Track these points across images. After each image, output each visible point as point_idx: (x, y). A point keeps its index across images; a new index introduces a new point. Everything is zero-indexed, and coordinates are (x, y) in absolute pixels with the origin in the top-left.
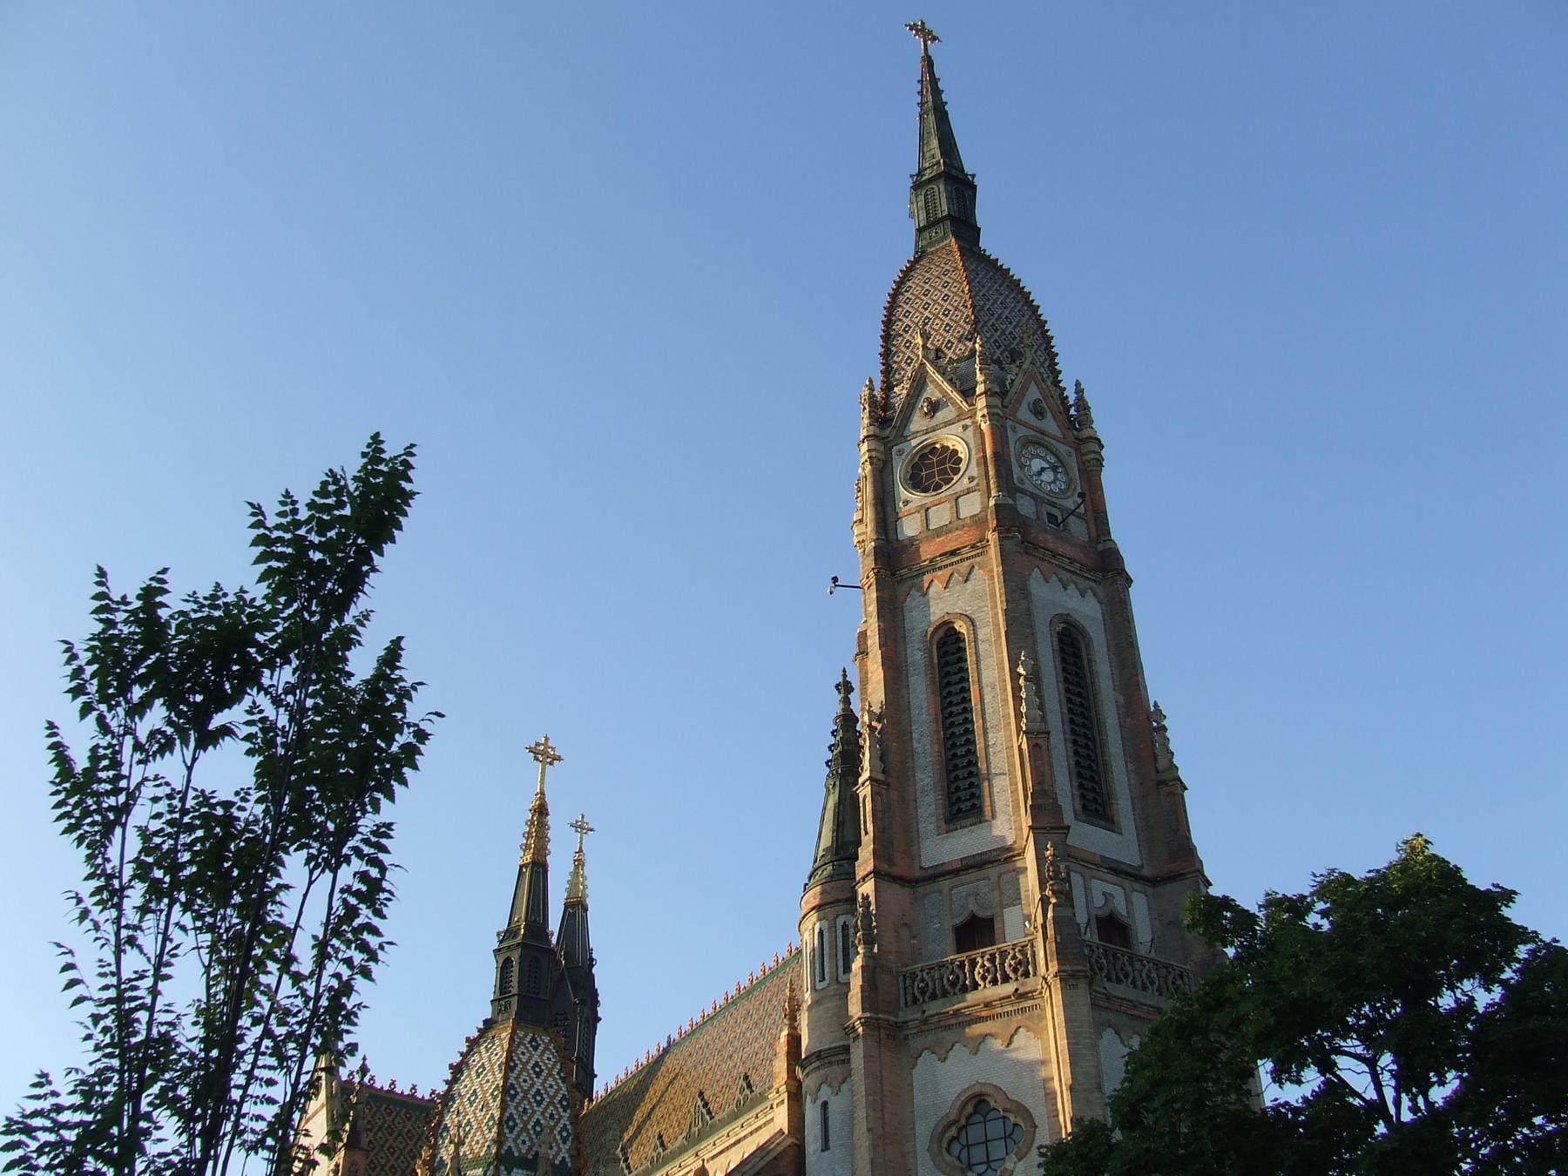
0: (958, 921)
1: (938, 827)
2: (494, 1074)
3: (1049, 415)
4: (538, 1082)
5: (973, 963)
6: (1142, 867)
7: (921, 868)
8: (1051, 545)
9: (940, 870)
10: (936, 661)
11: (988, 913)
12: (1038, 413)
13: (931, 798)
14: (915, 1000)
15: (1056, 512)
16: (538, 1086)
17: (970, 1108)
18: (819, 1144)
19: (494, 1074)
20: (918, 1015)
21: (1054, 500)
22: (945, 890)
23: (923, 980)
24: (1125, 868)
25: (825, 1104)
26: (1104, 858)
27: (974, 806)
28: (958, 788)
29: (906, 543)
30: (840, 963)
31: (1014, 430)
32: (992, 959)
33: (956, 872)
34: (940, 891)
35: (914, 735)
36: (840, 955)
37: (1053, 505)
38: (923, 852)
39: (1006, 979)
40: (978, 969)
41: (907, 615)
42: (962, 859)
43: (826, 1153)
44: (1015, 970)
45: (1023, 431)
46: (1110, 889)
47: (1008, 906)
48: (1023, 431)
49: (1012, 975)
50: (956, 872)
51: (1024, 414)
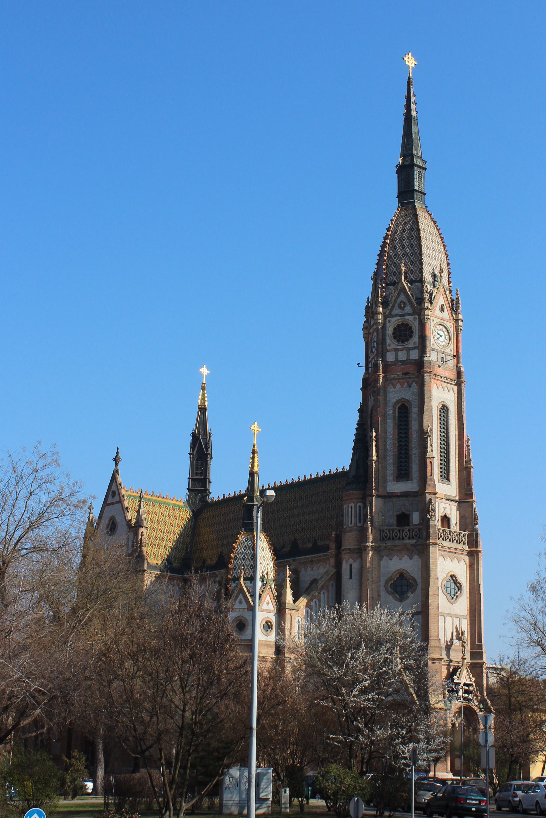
0: (398, 513)
1: (394, 479)
2: (250, 550)
4: (263, 553)
5: (403, 531)
6: (456, 496)
7: (387, 492)
10: (397, 415)
11: (408, 513)
12: (442, 310)
15: (444, 356)
16: (263, 555)
18: (348, 577)
19: (250, 550)
21: (443, 350)
22: (395, 502)
23: (386, 533)
24: (452, 498)
25: (351, 565)
26: (445, 495)
27: (406, 473)
28: (401, 465)
29: (390, 363)
30: (358, 520)
31: (433, 321)
32: (409, 531)
34: (393, 502)
35: (388, 443)
36: (358, 517)
37: (443, 353)
38: (388, 487)
39: (413, 538)
40: (404, 533)
41: (388, 394)
42: (401, 492)
43: (351, 580)
44: (416, 536)
45: (437, 320)
46: (445, 505)
47: (414, 512)
48: (437, 320)
49: (415, 537)
51: (437, 312)
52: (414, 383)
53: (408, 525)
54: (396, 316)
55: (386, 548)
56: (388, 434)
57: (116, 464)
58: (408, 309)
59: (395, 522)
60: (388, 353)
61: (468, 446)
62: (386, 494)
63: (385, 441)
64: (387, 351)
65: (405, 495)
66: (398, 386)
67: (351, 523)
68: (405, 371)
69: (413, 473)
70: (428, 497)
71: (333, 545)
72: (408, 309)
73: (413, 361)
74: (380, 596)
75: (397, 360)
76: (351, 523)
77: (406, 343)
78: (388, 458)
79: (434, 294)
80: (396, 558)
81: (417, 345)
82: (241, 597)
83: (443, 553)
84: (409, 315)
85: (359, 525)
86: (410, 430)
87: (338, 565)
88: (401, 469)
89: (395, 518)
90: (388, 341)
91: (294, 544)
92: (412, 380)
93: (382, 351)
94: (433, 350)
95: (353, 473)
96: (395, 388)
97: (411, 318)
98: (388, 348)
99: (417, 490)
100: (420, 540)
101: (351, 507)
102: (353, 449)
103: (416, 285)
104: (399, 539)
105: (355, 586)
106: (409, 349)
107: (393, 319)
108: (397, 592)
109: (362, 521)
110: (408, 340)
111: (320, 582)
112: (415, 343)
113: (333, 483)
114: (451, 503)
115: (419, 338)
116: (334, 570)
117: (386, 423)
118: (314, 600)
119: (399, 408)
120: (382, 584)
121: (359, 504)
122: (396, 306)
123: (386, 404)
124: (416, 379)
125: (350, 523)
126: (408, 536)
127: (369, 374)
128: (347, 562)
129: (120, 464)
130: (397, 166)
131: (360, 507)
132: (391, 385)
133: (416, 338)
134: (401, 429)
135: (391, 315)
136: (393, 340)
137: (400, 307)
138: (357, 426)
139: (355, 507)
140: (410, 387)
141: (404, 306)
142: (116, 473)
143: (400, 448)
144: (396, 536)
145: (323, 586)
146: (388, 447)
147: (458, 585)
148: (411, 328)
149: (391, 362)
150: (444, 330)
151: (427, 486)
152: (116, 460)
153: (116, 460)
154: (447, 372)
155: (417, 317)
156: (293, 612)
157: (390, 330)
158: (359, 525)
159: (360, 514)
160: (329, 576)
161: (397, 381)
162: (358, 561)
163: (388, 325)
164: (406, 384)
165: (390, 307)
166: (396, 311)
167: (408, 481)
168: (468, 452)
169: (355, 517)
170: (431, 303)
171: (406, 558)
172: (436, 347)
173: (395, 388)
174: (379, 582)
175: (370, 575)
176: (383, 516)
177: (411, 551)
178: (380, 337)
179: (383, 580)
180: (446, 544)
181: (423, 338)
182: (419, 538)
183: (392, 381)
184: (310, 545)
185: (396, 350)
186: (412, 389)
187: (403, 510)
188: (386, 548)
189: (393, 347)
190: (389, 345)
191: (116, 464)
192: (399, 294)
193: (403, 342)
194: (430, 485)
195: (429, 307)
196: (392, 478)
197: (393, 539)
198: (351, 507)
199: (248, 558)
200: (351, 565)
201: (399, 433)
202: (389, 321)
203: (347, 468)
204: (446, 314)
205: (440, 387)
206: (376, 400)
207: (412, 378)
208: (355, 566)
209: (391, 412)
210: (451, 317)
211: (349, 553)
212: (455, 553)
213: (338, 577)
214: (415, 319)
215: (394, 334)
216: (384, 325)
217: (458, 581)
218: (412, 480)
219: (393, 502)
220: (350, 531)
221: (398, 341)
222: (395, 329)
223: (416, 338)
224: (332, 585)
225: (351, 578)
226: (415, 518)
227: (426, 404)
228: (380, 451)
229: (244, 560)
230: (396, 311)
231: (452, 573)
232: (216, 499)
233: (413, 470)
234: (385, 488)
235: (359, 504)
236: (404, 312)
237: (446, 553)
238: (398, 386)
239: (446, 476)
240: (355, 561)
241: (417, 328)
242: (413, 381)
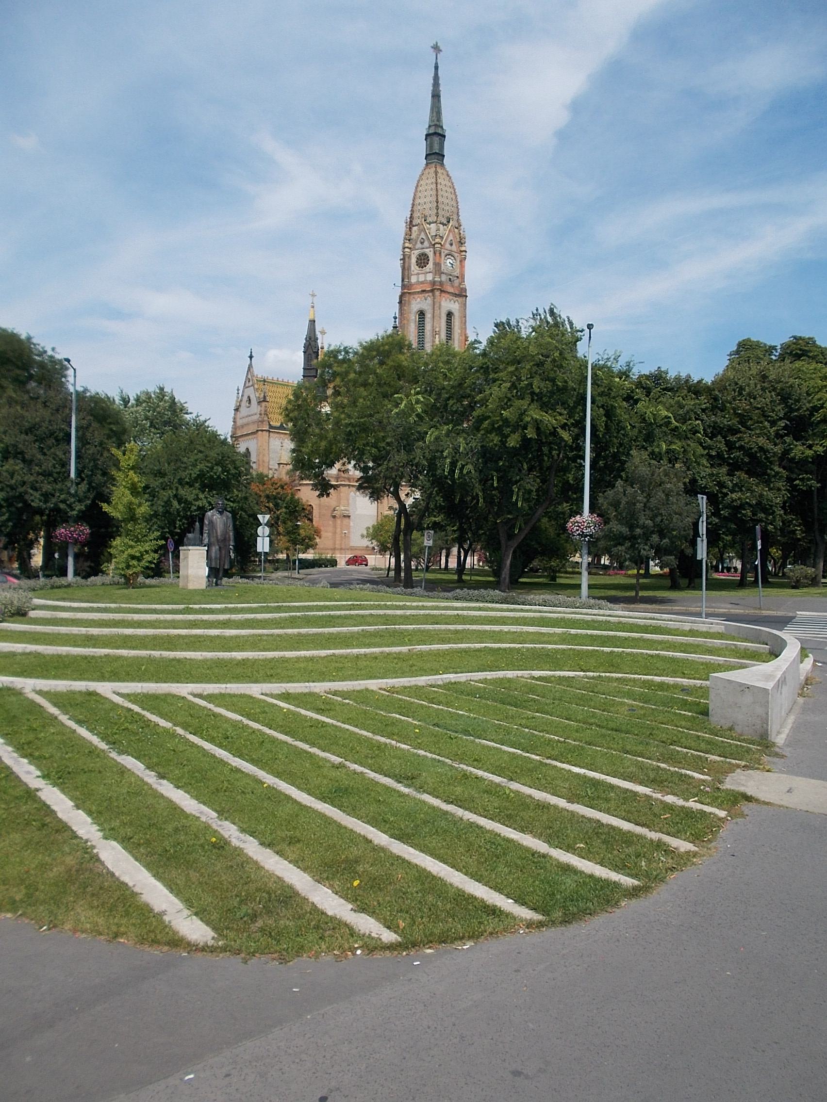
12: (451, 245)
15: (451, 277)
45: (447, 252)
51: (448, 246)
57: (251, 360)
58: (426, 244)
72: (426, 244)
84: (427, 248)
90: (412, 268)
122: (419, 242)
129: (253, 359)
133: (430, 265)
142: (250, 366)
152: (251, 357)
153: (251, 357)
157: (414, 260)
163: (412, 256)
166: (419, 245)
185: (418, 274)
189: (416, 272)
191: (251, 360)
209: (413, 318)
215: (417, 262)
230: (419, 245)
236: (423, 246)
238: (419, 299)
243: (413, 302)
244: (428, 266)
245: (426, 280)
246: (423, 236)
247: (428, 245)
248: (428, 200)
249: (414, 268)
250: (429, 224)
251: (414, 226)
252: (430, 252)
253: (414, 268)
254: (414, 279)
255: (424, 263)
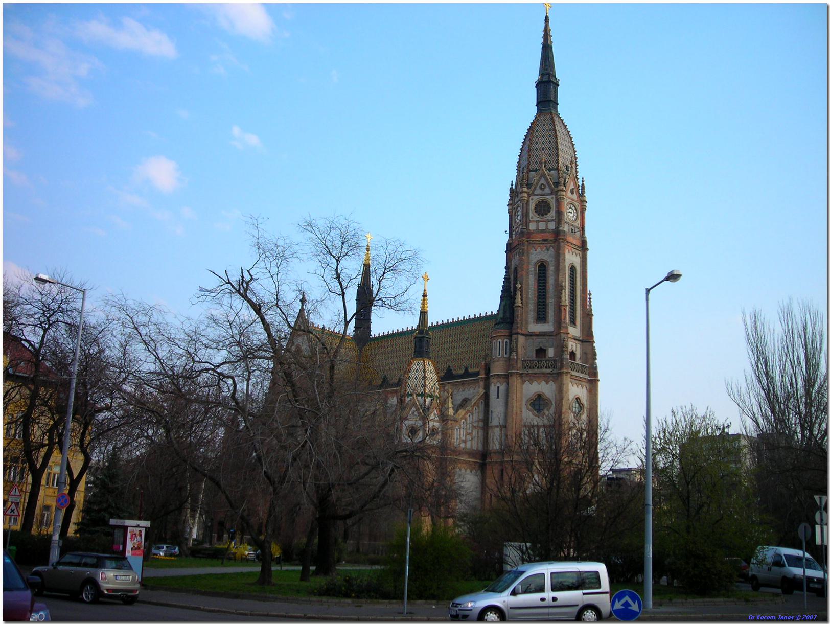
0: (537, 348)
1: (534, 321)
3: (575, 193)
8: (571, 241)
9: (534, 333)
11: (545, 348)
12: (572, 193)
13: (532, 313)
14: (525, 368)
17: (536, 397)
18: (496, 396)
20: (526, 372)
24: (577, 338)
25: (498, 387)
26: (573, 336)
27: (543, 317)
33: (537, 335)
35: (530, 293)
38: (529, 327)
39: (549, 368)
44: (552, 366)
45: (569, 200)
50: (537, 335)
51: (569, 194)
52: (551, 248)
53: (545, 357)
54: (537, 195)
55: (528, 374)
56: (530, 286)
58: (547, 190)
59: (534, 355)
60: (531, 223)
61: (590, 299)
62: (527, 333)
63: (528, 292)
64: (530, 222)
65: (542, 334)
66: (539, 249)
67: (499, 355)
68: (544, 238)
69: (550, 317)
70: (563, 336)
71: (483, 372)
72: (547, 190)
73: (551, 231)
74: (522, 412)
75: (538, 229)
76: (499, 355)
77: (545, 216)
78: (530, 305)
79: (567, 180)
80: (535, 383)
81: (554, 218)
82: (414, 409)
83: (572, 380)
84: (548, 194)
85: (505, 356)
86: (547, 284)
87: (487, 387)
88: (540, 314)
89: (534, 352)
90: (531, 215)
91: (449, 370)
92: (549, 245)
93: (526, 221)
94: (566, 223)
95: (501, 316)
96: (536, 251)
97: (549, 197)
98: (531, 219)
99: (553, 330)
100: (555, 370)
101: (500, 342)
102: (501, 298)
103: (553, 172)
104: (538, 368)
105: (501, 404)
106: (549, 221)
107: (535, 198)
108: (535, 410)
109: (508, 353)
110: (547, 214)
111: (473, 400)
112: (552, 217)
113: (478, 325)
114: (577, 342)
115: (556, 213)
116: (484, 391)
117: (529, 278)
118: (469, 414)
119: (539, 267)
120: (524, 403)
121: (505, 340)
122: (538, 187)
123: (529, 263)
124: (553, 245)
125: (498, 354)
126: (545, 366)
127: (512, 240)
128: (495, 386)
130: (536, 82)
131: (506, 342)
132: (533, 249)
133: (552, 214)
134: (540, 283)
135: (534, 195)
136: (535, 214)
137: (541, 188)
138: (504, 280)
139: (503, 342)
140: (548, 250)
141: (544, 189)
143: (539, 297)
144: (536, 366)
145: (475, 403)
146: (530, 296)
147: (581, 405)
148: (549, 204)
149: (534, 230)
150: (574, 208)
151: (562, 328)
154: (575, 241)
155: (554, 196)
156: (453, 422)
157: (532, 206)
158: (505, 356)
159: (506, 348)
160: (480, 396)
161: (538, 245)
162: (505, 384)
163: (531, 202)
164: (545, 248)
165: (532, 188)
166: (538, 191)
167: (545, 323)
168: (590, 303)
169: (503, 350)
170: (565, 186)
171: (544, 383)
172: (568, 221)
173: (536, 251)
174: (521, 400)
175: (515, 395)
176: (525, 350)
177: (546, 377)
178: (525, 211)
179: (524, 400)
180: (573, 373)
181: (559, 213)
182: (554, 368)
183: (534, 245)
184: (462, 372)
185: (537, 222)
186: (550, 252)
187: (541, 345)
188: (528, 374)
189: (535, 219)
190: (532, 218)
192: (540, 178)
193: (543, 215)
194: (563, 327)
195: (564, 189)
196: (532, 321)
197: (533, 368)
198: (500, 342)
199: (419, 379)
200: (498, 387)
201: (539, 286)
202: (532, 199)
203: (495, 312)
204: (575, 197)
205: (571, 252)
206: (521, 260)
207: (550, 243)
208: (502, 388)
209: (533, 269)
210: (579, 198)
211: (497, 378)
212: (580, 381)
213: (486, 397)
214: (552, 198)
215: (535, 209)
216: (528, 201)
217: (582, 402)
218: (548, 323)
219: (533, 339)
220: (498, 361)
221: (539, 215)
222: (536, 205)
223: (552, 214)
224: (482, 402)
225: (498, 397)
226: (551, 352)
227: (561, 264)
228: (524, 299)
229: (416, 380)
230: (538, 191)
231: (577, 396)
232: (377, 335)
233: (550, 315)
234: (527, 328)
235: (505, 340)
236: (544, 193)
237: (573, 380)
238: (539, 249)
239: (573, 322)
240: (502, 385)
241: (554, 205)
242: (551, 246)
243: (532, 251)
244: (549, 214)
245: (547, 229)
246: (543, 181)
247: (550, 192)
248: (547, 145)
249: (533, 215)
250: (550, 170)
251: (530, 171)
252: (551, 199)
253: (533, 215)
254: (532, 227)
255: (544, 207)
